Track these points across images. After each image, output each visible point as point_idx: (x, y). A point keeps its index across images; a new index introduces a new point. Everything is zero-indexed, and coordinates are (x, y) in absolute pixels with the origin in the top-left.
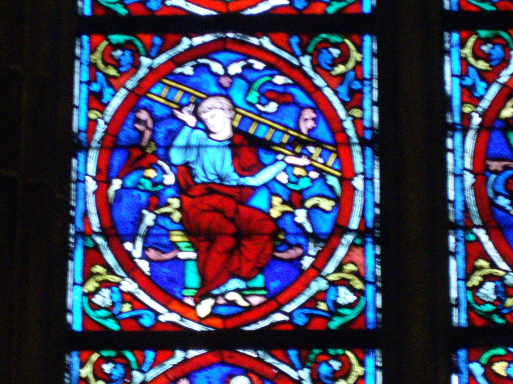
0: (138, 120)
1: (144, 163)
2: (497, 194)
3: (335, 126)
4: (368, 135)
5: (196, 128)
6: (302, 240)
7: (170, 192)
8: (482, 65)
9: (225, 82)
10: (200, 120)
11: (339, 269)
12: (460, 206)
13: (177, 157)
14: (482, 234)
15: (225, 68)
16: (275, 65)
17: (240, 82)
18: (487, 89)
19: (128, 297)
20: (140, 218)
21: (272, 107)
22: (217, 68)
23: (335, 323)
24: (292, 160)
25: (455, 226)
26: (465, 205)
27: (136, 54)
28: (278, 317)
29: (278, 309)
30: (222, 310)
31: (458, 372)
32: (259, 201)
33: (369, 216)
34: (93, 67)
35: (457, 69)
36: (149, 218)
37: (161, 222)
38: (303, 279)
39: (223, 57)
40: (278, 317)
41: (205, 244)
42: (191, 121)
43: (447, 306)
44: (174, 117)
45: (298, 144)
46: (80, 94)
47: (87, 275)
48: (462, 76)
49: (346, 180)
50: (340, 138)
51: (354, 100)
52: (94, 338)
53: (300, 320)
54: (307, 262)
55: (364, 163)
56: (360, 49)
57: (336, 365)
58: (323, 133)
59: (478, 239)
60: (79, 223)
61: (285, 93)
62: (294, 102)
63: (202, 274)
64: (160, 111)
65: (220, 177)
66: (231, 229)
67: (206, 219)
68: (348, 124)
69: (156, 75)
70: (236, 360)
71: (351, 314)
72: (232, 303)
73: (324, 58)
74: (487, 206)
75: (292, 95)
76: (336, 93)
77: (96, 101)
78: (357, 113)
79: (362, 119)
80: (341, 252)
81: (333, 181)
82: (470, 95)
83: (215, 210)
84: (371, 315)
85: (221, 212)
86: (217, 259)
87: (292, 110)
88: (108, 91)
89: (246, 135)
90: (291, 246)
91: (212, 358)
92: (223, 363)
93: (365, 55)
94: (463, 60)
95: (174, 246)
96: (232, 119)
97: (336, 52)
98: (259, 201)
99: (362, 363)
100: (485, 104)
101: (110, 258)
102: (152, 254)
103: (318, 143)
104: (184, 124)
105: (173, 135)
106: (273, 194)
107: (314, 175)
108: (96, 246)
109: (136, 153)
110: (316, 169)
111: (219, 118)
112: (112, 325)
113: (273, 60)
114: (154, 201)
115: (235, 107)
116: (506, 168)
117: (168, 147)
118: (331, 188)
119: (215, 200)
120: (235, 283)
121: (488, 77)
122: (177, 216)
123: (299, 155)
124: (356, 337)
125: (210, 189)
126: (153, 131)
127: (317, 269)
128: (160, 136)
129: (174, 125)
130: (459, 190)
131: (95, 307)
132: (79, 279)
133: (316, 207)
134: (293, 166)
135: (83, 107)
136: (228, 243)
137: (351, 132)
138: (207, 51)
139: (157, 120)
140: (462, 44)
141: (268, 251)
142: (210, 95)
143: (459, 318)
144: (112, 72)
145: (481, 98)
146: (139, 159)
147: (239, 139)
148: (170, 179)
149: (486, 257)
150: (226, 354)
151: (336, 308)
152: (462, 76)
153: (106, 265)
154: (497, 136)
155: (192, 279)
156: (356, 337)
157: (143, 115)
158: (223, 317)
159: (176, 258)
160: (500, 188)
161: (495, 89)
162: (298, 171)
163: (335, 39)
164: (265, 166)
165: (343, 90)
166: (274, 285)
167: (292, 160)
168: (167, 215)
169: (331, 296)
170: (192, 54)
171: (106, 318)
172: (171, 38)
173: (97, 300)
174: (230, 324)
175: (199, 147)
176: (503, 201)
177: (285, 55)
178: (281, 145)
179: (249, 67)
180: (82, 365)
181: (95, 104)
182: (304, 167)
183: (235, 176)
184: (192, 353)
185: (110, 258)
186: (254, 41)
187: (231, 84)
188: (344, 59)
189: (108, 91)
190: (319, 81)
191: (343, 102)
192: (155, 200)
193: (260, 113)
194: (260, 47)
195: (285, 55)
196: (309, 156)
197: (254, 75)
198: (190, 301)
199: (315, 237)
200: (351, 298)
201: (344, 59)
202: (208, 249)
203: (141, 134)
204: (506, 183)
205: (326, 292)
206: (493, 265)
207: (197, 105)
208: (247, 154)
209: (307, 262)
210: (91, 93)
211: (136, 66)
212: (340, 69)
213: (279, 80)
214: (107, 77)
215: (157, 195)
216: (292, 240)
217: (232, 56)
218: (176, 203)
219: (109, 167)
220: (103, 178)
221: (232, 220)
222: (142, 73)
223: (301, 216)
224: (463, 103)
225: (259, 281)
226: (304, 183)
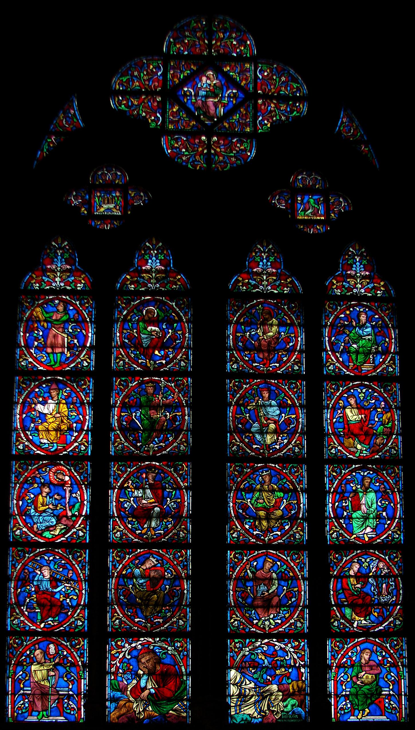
0: (25, 572)
1: (26, 584)
2: (120, 595)
3: (78, 575)
4: (87, 578)
5: (40, 575)
6: (68, 607)
7: (33, 593)
8: (118, 559)
9: (48, 562)
10: (41, 573)
11: (78, 615)
12: (110, 599)
13: (35, 583)
14: (116, 606)
15: (49, 558)
16: (62, 557)
17: (52, 562)
18: (119, 566)
19: (23, 622)
20: (26, 600)
21: (61, 569)
22: (46, 558)
23: (77, 630)
24: (66, 585)
25: (109, 604)
26: (112, 598)
27: (25, 553)
28: (62, 628)
29: (62, 626)
30: (47, 626)
31: (109, 644)
32: (57, 596)
33: (86, 601)
34: (13, 556)
35: (111, 559)
36: (28, 600)
37: (31, 601)
38: (68, 618)
39: (48, 555)
40: (62, 628)
41: (42, 608)
42: (39, 573)
43: (107, 626)
44: (35, 572)
45: (68, 580)
46: (10, 565)
47: (12, 615)
48: (112, 562)
49: (80, 591)
50: (79, 579)
51: (83, 569)
52: (14, 633)
53: (67, 629)
54: (69, 613)
55: (85, 586)
56: (85, 554)
57: (77, 641)
58: (75, 577)
59: (115, 608)
60: (9, 601)
61: (64, 566)
62: (67, 568)
63: (41, 616)
64: (31, 570)
65: (46, 589)
66: (49, 604)
67: (43, 601)
68: (81, 575)
69: (30, 559)
70: (51, 640)
71: (81, 628)
72: (50, 624)
73: (76, 556)
74: (118, 599)
75: (67, 566)
76: (78, 566)
77: (14, 566)
78: (84, 572)
79: (85, 573)
80: (79, 611)
81: (77, 591)
82: (114, 567)
83: (45, 598)
84: (86, 628)
85: (47, 599)
86: (45, 612)
87: (67, 571)
88: (17, 564)
89: (54, 577)
90: (66, 609)
91: (44, 639)
92: (47, 640)
93: (86, 556)
94: (113, 557)
95: (34, 608)
96: (50, 573)
97: (79, 554)
98: (57, 596)
99: (84, 641)
100: (118, 570)
101: (17, 611)
102: (28, 610)
103: (73, 580)
104: (37, 574)
105: (34, 577)
106: (61, 594)
107: (72, 589)
108: (14, 608)
109: (24, 582)
110: (72, 587)
111: (47, 573)
112: (18, 629)
113: (61, 556)
114: (29, 595)
115: (51, 569)
116: (123, 588)
117: (33, 580)
118: (76, 593)
119: (45, 596)
120: (50, 619)
121: (120, 562)
122: (35, 600)
123: (68, 584)
124: (82, 634)
125: (44, 592)
126: (29, 576)
127: (72, 616)
128: (31, 577)
129: (35, 574)
130: (111, 595)
131: (14, 624)
132: (9, 616)
133: (72, 598)
134: (67, 586)
135: (10, 568)
136: (49, 608)
137: (82, 577)
138: (44, 553)
139: (30, 573)
140: (113, 553)
141: (59, 610)
142: (44, 566)
143: (109, 629)
144: (18, 558)
145: (118, 568)
146: (25, 583)
147: (51, 579)
148: (33, 589)
149: (117, 613)
150: (48, 638)
151: (77, 626)
152: (112, 562)
153: (16, 612)
154: (121, 580)
155: (39, 617)
156: (82, 634)
157: (26, 571)
158: (47, 628)
159: (35, 611)
160: (121, 593)
161: (121, 566)
162: (67, 588)
163: (79, 550)
164: (59, 586)
165: (80, 565)
166: (61, 620)
167: (66, 585)
168: (33, 599)
169: (76, 623)
170: (40, 553)
171: (17, 627)
172: (34, 549)
173: (14, 622)
174: (49, 630)
175: (41, 580)
176: (122, 597)
177: (65, 555)
178: (63, 580)
179: (54, 558)
180: (10, 640)
181: (13, 567)
182: (69, 587)
183: (51, 589)
184: (39, 637)
185: (17, 611)
186: (57, 550)
187: (50, 563)
188: (81, 556)
189: (17, 564)
190: (74, 563)
191: (80, 568)
192: (30, 595)
193: (58, 571)
194: (58, 552)
195: (65, 555)
196: (71, 584)
197: (57, 560)
198: (38, 623)
199: (72, 607)
200: (81, 623)
201: (81, 556)
202: (43, 609)
203: (26, 576)
204: (123, 592)
205: (74, 622)
206: (118, 615)
207: (41, 567)
208: (54, 583)
209: (69, 613)
210: (12, 564)
211: (25, 557)
212: (80, 559)
213: (63, 562)
214: (17, 559)
215: (30, 593)
216: (66, 607)
217: (51, 555)
218: (35, 596)
219: (17, 585)
220: (15, 588)
221: (50, 601)
222: (26, 559)
223: (68, 600)
224: (112, 570)
225: (57, 618)
226: (69, 591)
